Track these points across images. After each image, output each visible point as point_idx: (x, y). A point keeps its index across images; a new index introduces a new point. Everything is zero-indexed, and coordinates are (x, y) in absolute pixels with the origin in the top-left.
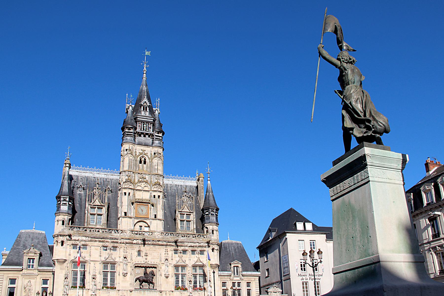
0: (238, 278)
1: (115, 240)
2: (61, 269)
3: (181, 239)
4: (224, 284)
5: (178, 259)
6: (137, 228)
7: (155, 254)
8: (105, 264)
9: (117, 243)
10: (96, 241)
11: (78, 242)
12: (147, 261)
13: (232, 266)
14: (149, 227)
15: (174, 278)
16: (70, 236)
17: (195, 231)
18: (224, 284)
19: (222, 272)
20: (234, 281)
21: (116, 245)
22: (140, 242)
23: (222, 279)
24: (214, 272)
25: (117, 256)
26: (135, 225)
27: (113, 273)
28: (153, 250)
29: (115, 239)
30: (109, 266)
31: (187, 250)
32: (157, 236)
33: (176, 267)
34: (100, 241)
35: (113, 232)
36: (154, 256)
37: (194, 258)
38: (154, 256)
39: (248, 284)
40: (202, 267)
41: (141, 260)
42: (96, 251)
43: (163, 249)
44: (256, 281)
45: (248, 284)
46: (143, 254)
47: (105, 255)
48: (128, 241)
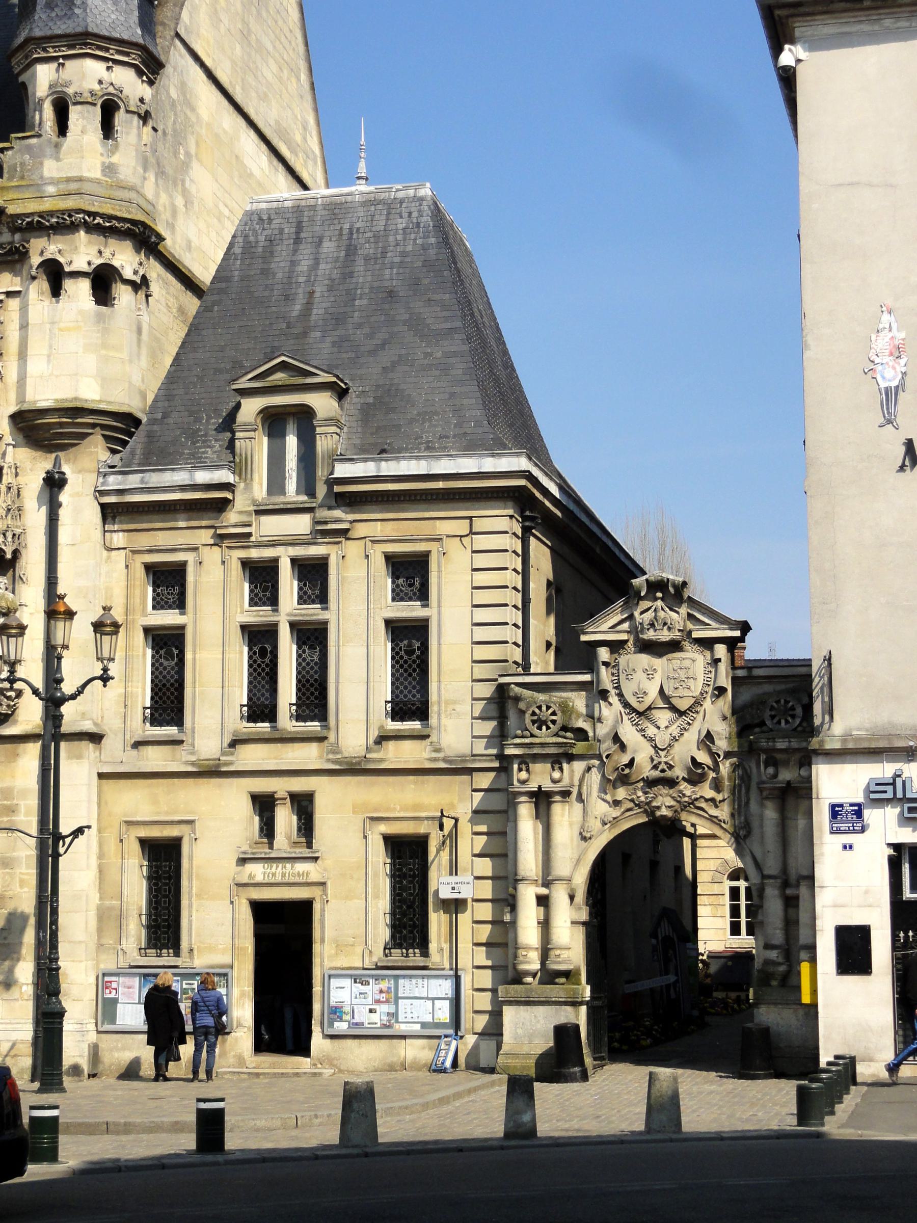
0: (301, 524)
4: (169, 581)
13: (251, 408)
18: (169, 581)
19: (133, 481)
20: (254, 554)
23: (145, 540)
24: (54, 483)
39: (410, 573)
44: (482, 542)
45: (410, 573)
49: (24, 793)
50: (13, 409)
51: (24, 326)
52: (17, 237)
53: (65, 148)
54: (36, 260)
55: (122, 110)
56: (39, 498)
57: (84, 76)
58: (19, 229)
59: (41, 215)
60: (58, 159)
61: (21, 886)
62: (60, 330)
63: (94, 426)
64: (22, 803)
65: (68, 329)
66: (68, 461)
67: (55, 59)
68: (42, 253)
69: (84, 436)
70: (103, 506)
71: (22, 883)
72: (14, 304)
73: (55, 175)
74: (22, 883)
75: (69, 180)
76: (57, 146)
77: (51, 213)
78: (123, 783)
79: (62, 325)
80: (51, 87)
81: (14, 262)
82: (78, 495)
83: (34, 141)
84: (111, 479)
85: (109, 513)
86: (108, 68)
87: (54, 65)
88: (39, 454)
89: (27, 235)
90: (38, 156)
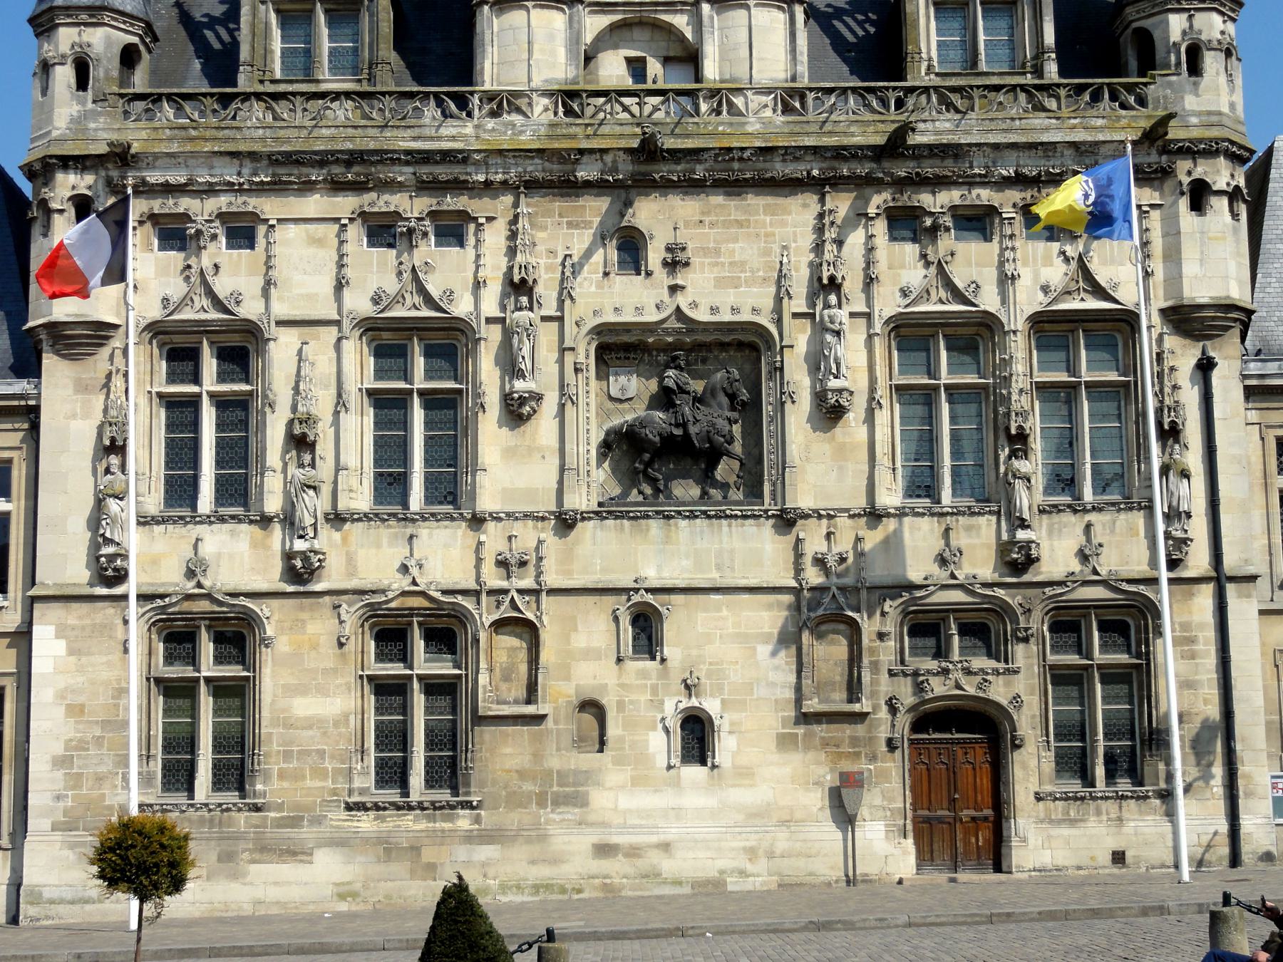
1: (444, 172)
2: (82, 388)
3: (933, 128)
5: (916, 276)
6: (613, 69)
7: (744, 250)
8: (387, 339)
9: (458, 186)
10: (307, 187)
11: (186, 204)
12: (682, 300)
14: (690, 58)
15: (889, 420)
16: (121, 157)
17: (1052, 70)
21: (452, 202)
22: (626, 168)
24: (1205, 367)
25: (461, 278)
26: (588, 59)
27: (444, 406)
28: (727, 224)
29: (447, 157)
30: (420, 354)
31: (992, 211)
32: (759, 121)
33: (910, 334)
34: (337, 187)
35: (431, 112)
36: (734, 260)
37: (1048, 262)
38: (734, 260)
40: (1116, 328)
41: (636, 300)
42: (312, 250)
43: (798, 214)
46: (655, 256)
47: (375, 272)
48: (535, 168)
49: (1202, 626)
50: (1165, 305)
51: (1173, 233)
52: (1164, 158)
53: (1202, 86)
54: (1186, 180)
55: (1234, 58)
56: (1191, 379)
57: (1211, 26)
58: (1169, 152)
59: (1190, 141)
60: (1197, 95)
61: (1205, 704)
62: (1209, 239)
63: (1235, 320)
64: (1200, 634)
65: (1216, 239)
66: (1214, 349)
67: (1189, 10)
68: (1189, 173)
69: (1228, 328)
70: (1246, 388)
71: (1206, 702)
72: (1155, 214)
73: (1196, 108)
74: (1206, 702)
75: (1209, 113)
76: (1196, 84)
77: (1201, 141)
78: (1273, 618)
79: (1211, 235)
80: (1184, 33)
81: (1154, 179)
82: (1225, 377)
83: (1174, 78)
84: (1252, 365)
85: (1250, 393)
86: (1224, 22)
87: (1185, 16)
88: (1188, 342)
89: (1173, 158)
90: (1179, 93)
